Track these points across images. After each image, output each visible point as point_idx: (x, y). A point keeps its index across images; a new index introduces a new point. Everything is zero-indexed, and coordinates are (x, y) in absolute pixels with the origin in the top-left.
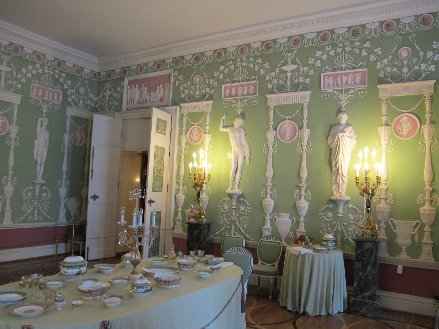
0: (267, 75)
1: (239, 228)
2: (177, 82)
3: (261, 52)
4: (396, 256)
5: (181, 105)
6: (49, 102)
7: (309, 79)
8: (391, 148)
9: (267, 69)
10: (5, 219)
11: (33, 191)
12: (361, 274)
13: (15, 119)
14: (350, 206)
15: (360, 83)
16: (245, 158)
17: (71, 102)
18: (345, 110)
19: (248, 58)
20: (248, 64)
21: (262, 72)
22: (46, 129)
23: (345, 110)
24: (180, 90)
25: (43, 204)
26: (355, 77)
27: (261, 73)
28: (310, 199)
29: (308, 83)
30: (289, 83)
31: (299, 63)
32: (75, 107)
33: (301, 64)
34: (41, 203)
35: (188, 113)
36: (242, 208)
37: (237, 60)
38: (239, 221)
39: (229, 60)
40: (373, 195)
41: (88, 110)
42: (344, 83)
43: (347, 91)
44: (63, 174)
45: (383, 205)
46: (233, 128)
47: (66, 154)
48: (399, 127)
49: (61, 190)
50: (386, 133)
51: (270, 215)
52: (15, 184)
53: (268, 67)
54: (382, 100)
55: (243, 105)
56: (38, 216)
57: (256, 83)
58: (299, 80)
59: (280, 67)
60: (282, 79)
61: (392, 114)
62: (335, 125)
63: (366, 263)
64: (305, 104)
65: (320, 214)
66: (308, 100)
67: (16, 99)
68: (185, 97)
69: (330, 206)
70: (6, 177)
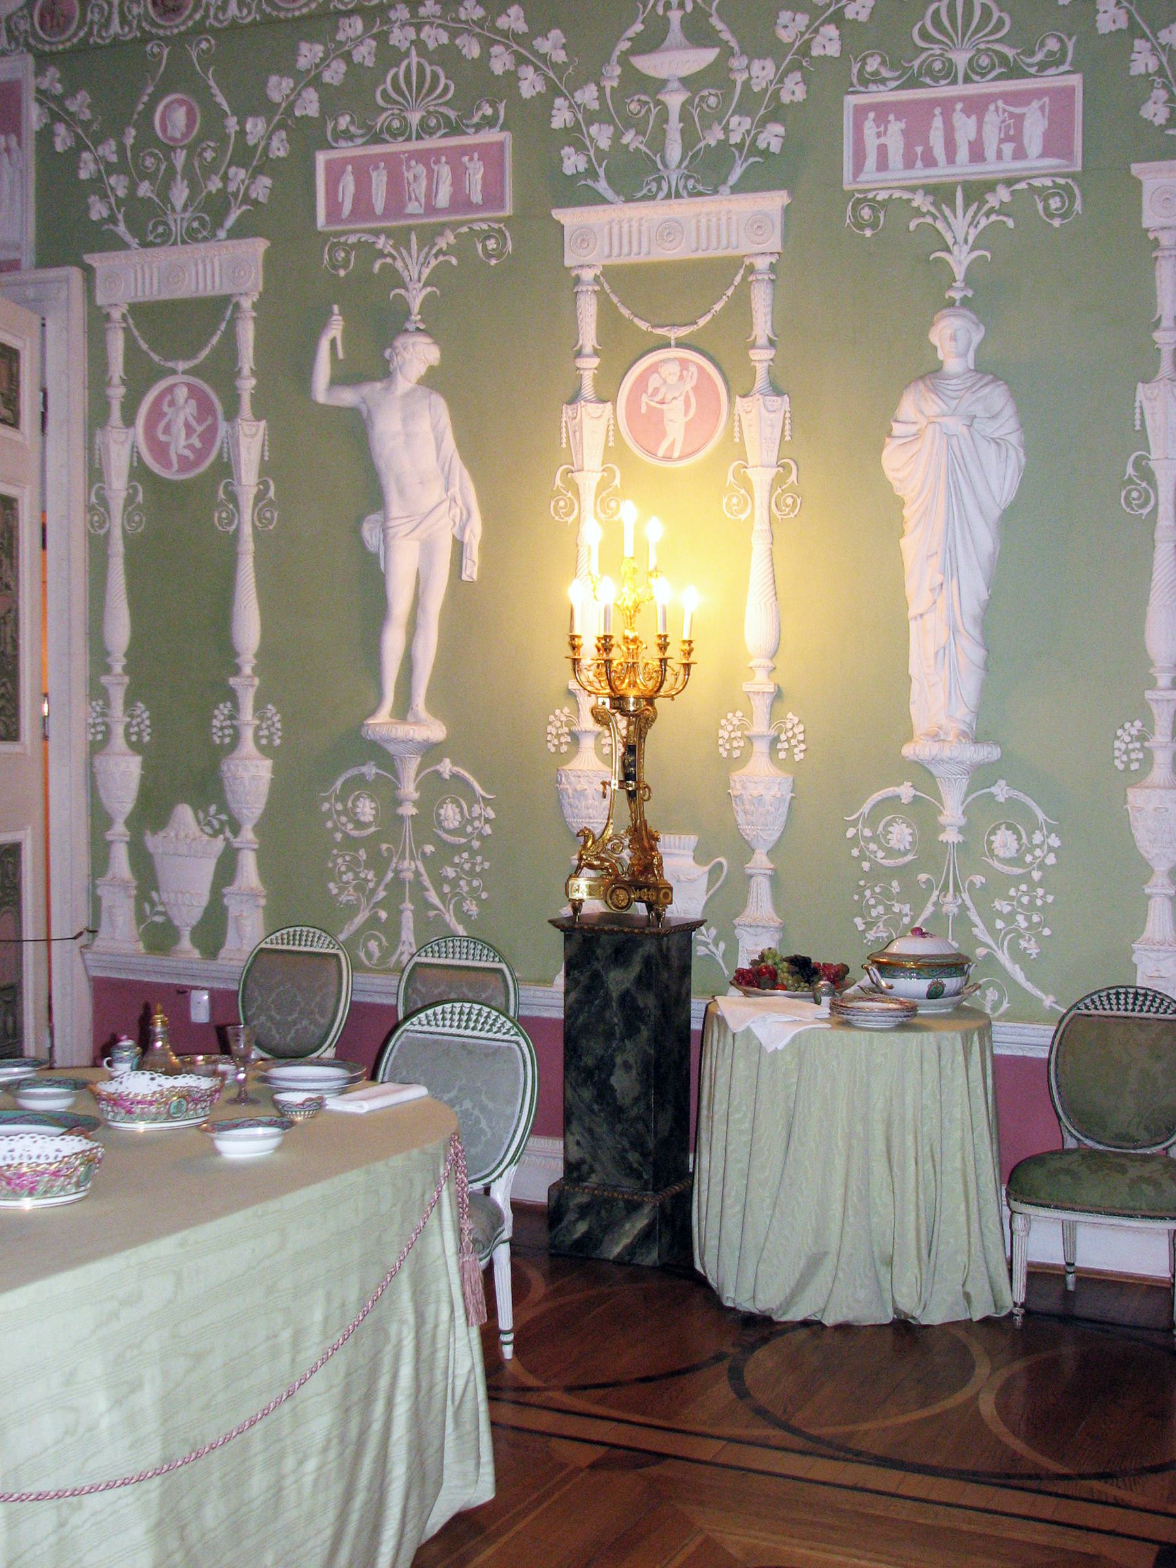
0: (559, 102)
1: (439, 918)
2: (61, 129)
5: (88, 258)
9: (554, 66)
16: (459, 547)
21: (530, 85)
24: (84, 175)
26: (1020, 118)
29: (775, 147)
30: (674, 151)
31: (726, 36)
33: (733, 43)
36: (450, 814)
37: (393, 15)
38: (439, 881)
53: (560, 56)
57: (501, 145)
58: (726, 129)
59: (624, 60)
68: (112, 219)
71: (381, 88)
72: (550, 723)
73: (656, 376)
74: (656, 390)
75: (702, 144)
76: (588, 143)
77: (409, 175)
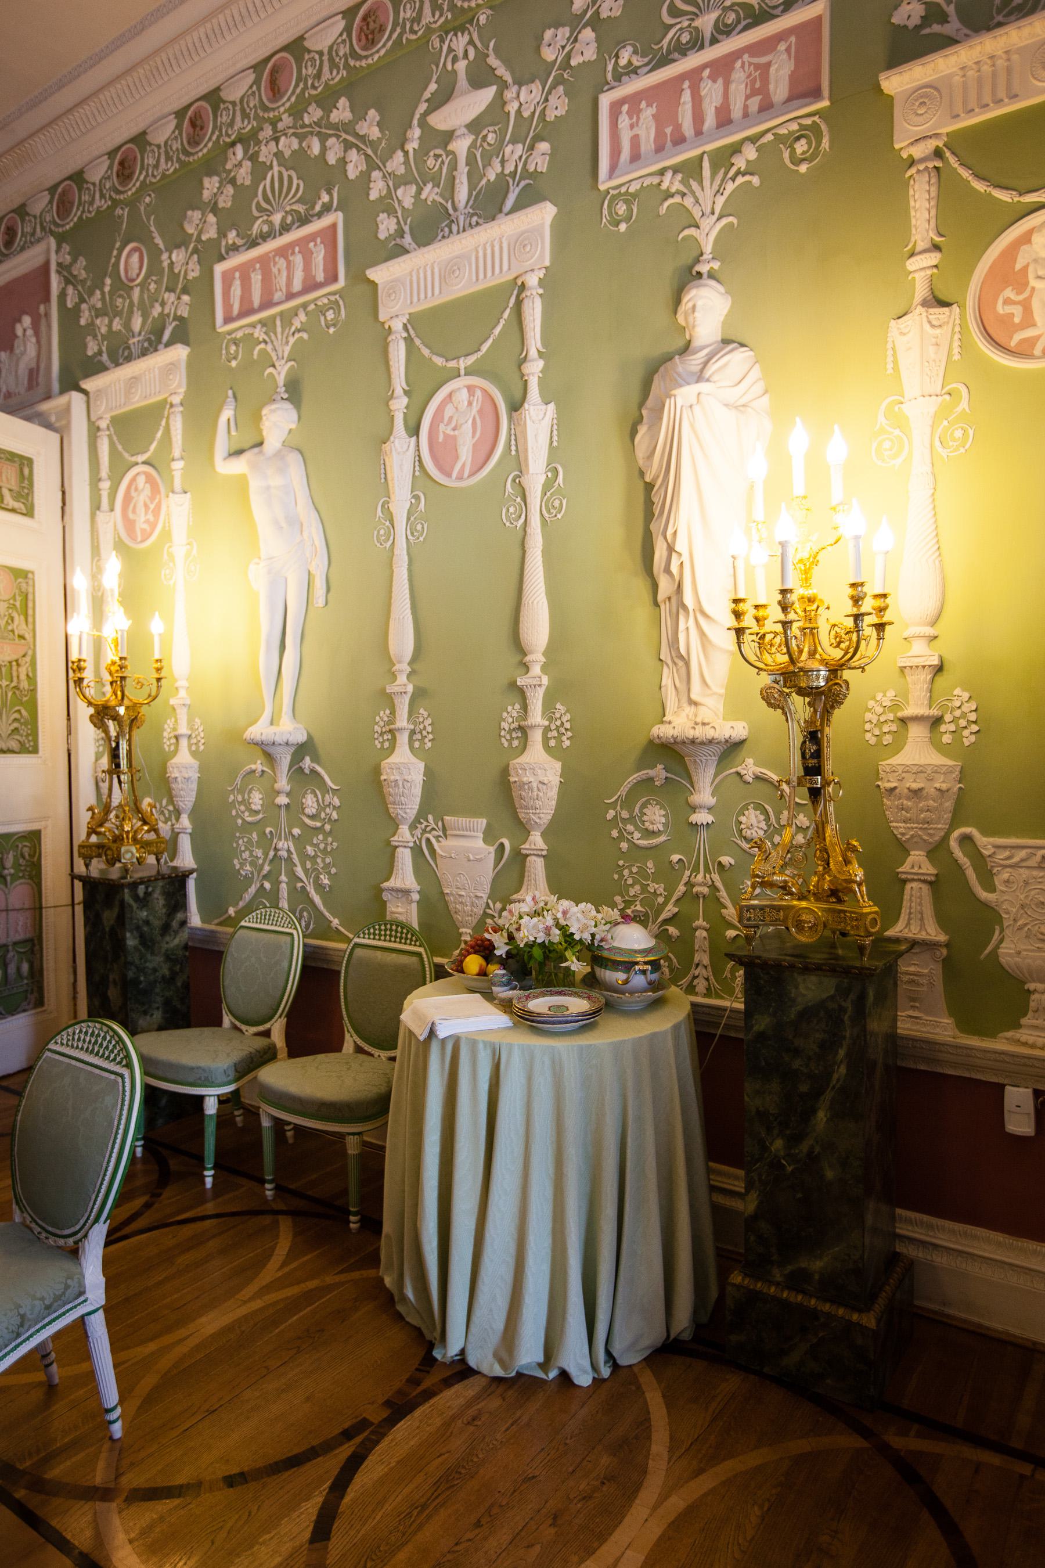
0: (376, 174)
2: (70, 290)
3: (347, 65)
4: (993, 1035)
5: (86, 385)
7: (544, 146)
8: (958, 434)
12: (778, 1145)
14: (749, 767)
15: (789, 100)
18: (716, 265)
19: (297, 112)
20: (300, 144)
23: (716, 265)
27: (352, 173)
28: (567, 743)
30: (462, 193)
31: (502, 71)
33: (508, 77)
35: (115, 421)
36: (310, 803)
37: (262, 136)
38: (304, 857)
39: (233, 144)
40: (828, 698)
42: (710, 121)
43: (723, 159)
45: (917, 753)
46: (261, 452)
48: (1008, 302)
50: (931, 350)
51: (413, 827)
53: (375, 133)
54: (912, 162)
55: (292, 340)
57: (334, 226)
58: (503, 162)
59: (423, 124)
60: (432, 180)
61: (968, 228)
62: (668, 358)
63: (804, 1088)
64: (532, 280)
65: (611, 814)
66: (542, 254)
68: (100, 353)
69: (651, 773)
71: (256, 200)
72: (377, 723)
73: (450, 405)
74: (451, 418)
75: (484, 182)
76: (396, 205)
77: (275, 270)
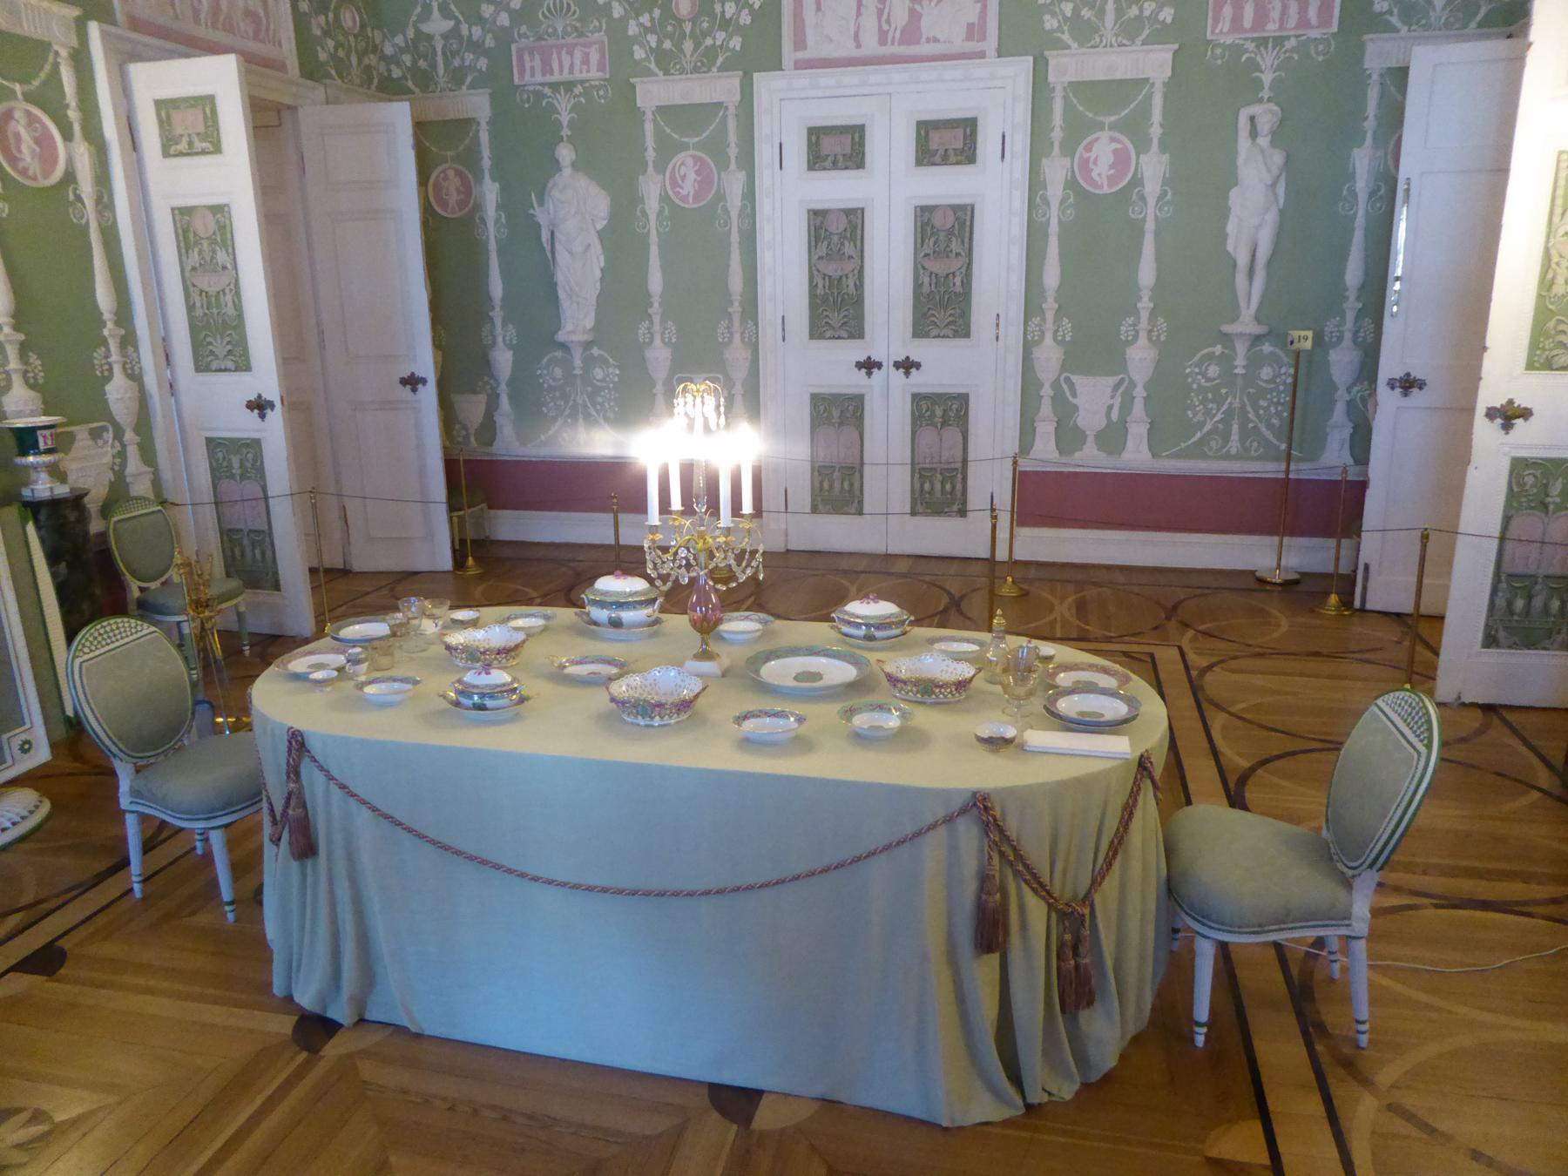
6: (1288, 38)
10: (1130, 443)
11: (1226, 361)
13: (1156, 131)
17: (1390, 12)
22: (1273, 144)
25: (1263, 403)
32: (1404, 29)
34: (1254, 400)
41: (1473, 24)
44: (1346, 298)
47: (1360, 221)
49: (1334, 355)
52: (1163, 338)
56: (1242, 440)
67: (1155, 63)
70: (1131, 320)
